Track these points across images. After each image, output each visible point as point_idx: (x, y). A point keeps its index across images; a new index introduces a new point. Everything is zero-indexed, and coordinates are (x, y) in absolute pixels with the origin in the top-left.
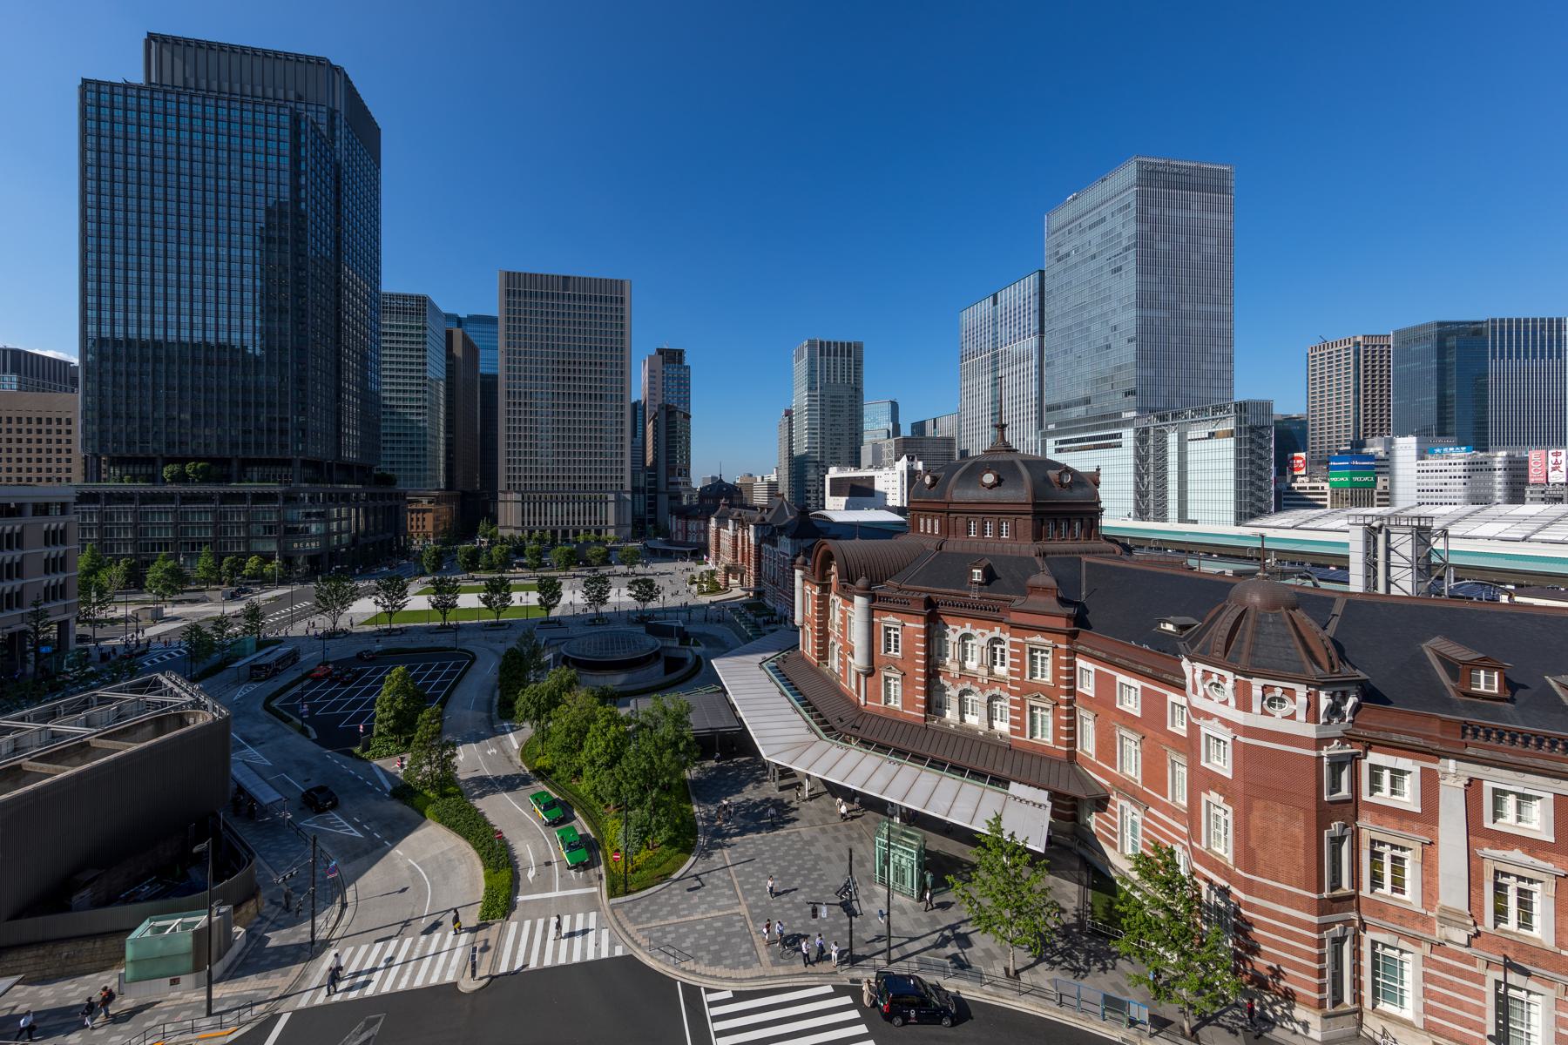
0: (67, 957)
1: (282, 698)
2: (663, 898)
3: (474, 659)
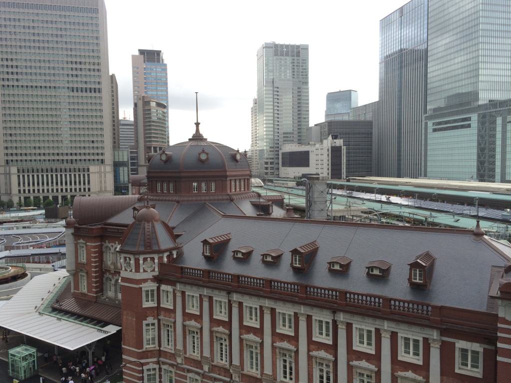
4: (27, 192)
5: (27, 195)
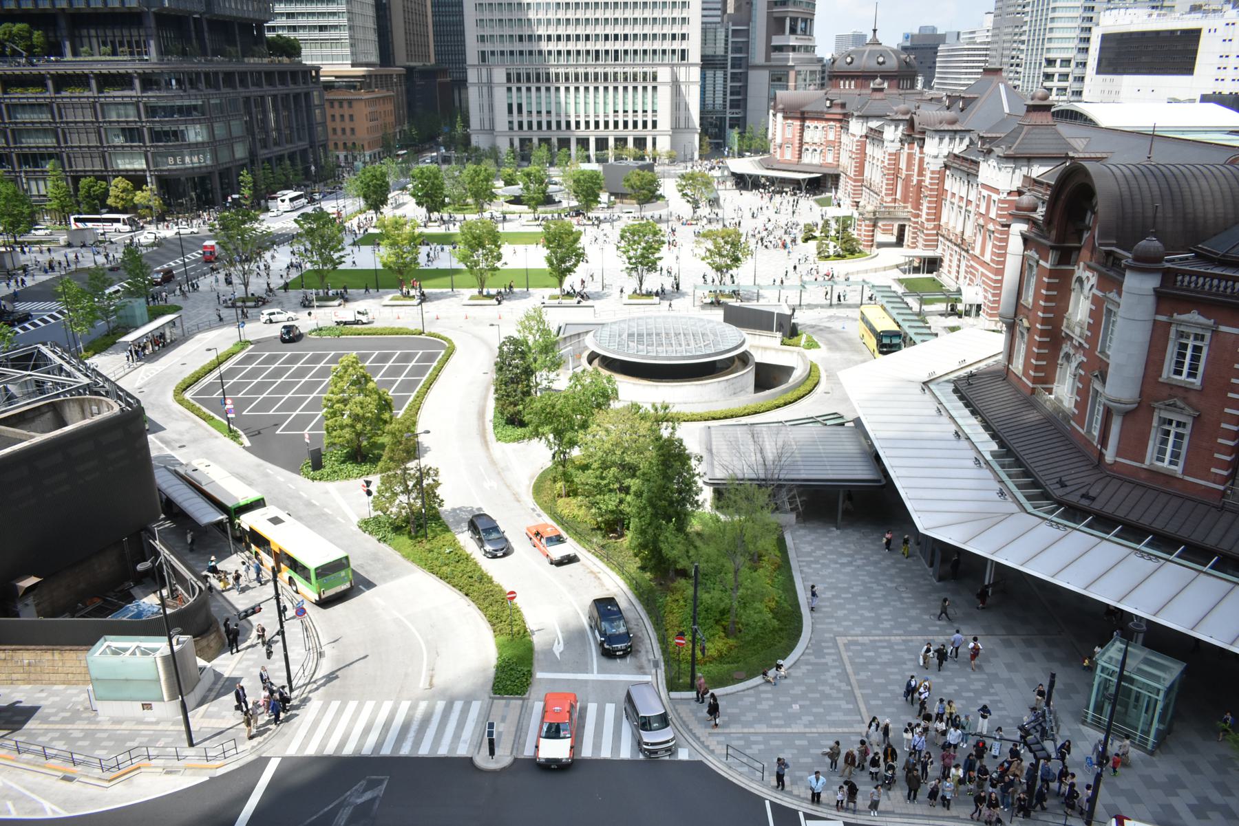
0: (29, 664)
1: (197, 388)
2: (748, 701)
3: (450, 351)
4: (525, 127)
5: (525, 133)
